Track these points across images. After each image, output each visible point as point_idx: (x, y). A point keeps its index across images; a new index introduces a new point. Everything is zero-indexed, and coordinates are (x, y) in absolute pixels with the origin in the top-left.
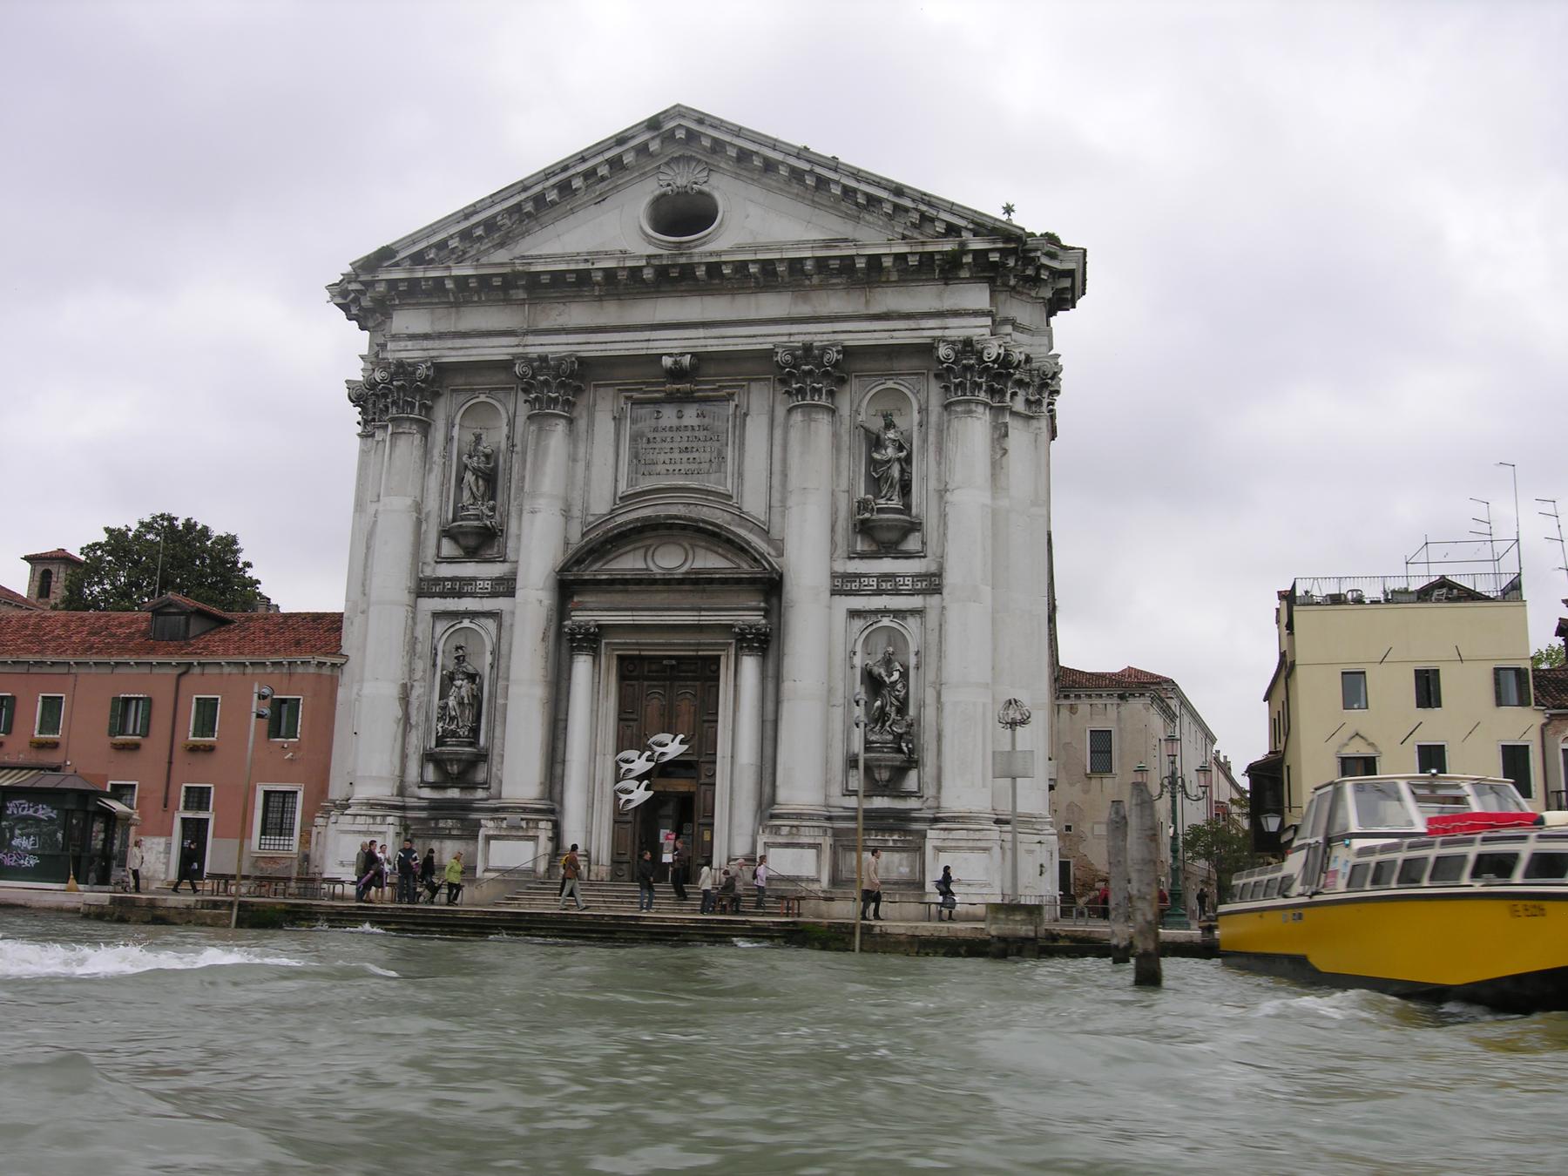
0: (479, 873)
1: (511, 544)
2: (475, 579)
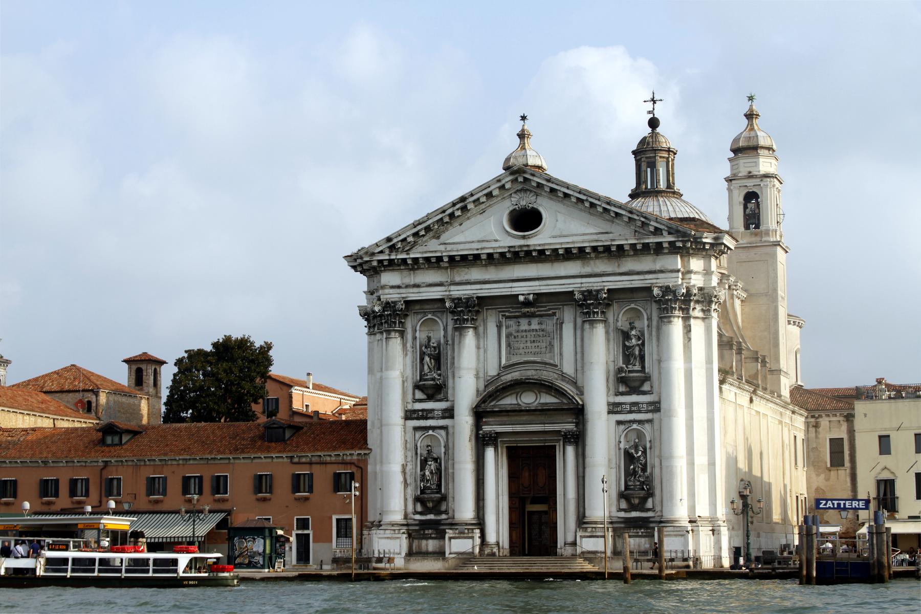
0: (447, 555)
1: (450, 391)
2: (433, 410)
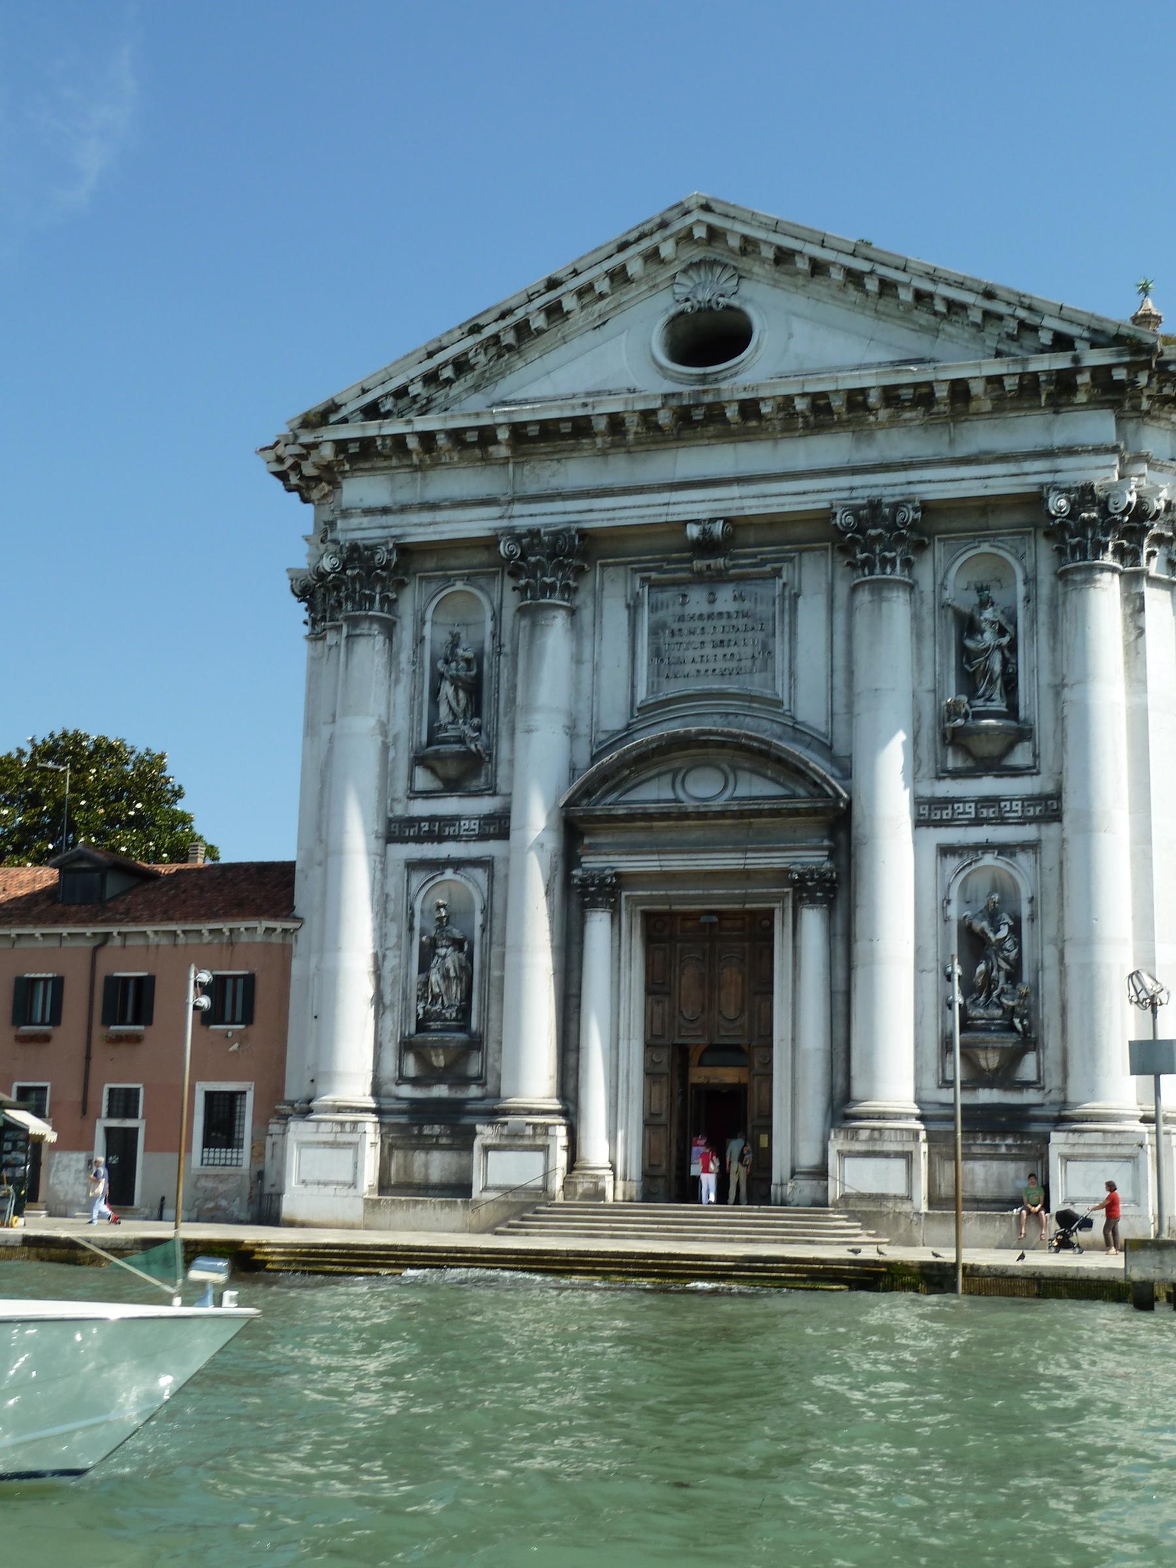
0: (476, 1193)
1: (502, 771)
2: (454, 819)
